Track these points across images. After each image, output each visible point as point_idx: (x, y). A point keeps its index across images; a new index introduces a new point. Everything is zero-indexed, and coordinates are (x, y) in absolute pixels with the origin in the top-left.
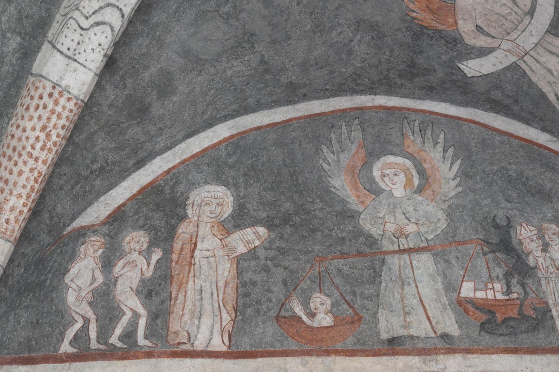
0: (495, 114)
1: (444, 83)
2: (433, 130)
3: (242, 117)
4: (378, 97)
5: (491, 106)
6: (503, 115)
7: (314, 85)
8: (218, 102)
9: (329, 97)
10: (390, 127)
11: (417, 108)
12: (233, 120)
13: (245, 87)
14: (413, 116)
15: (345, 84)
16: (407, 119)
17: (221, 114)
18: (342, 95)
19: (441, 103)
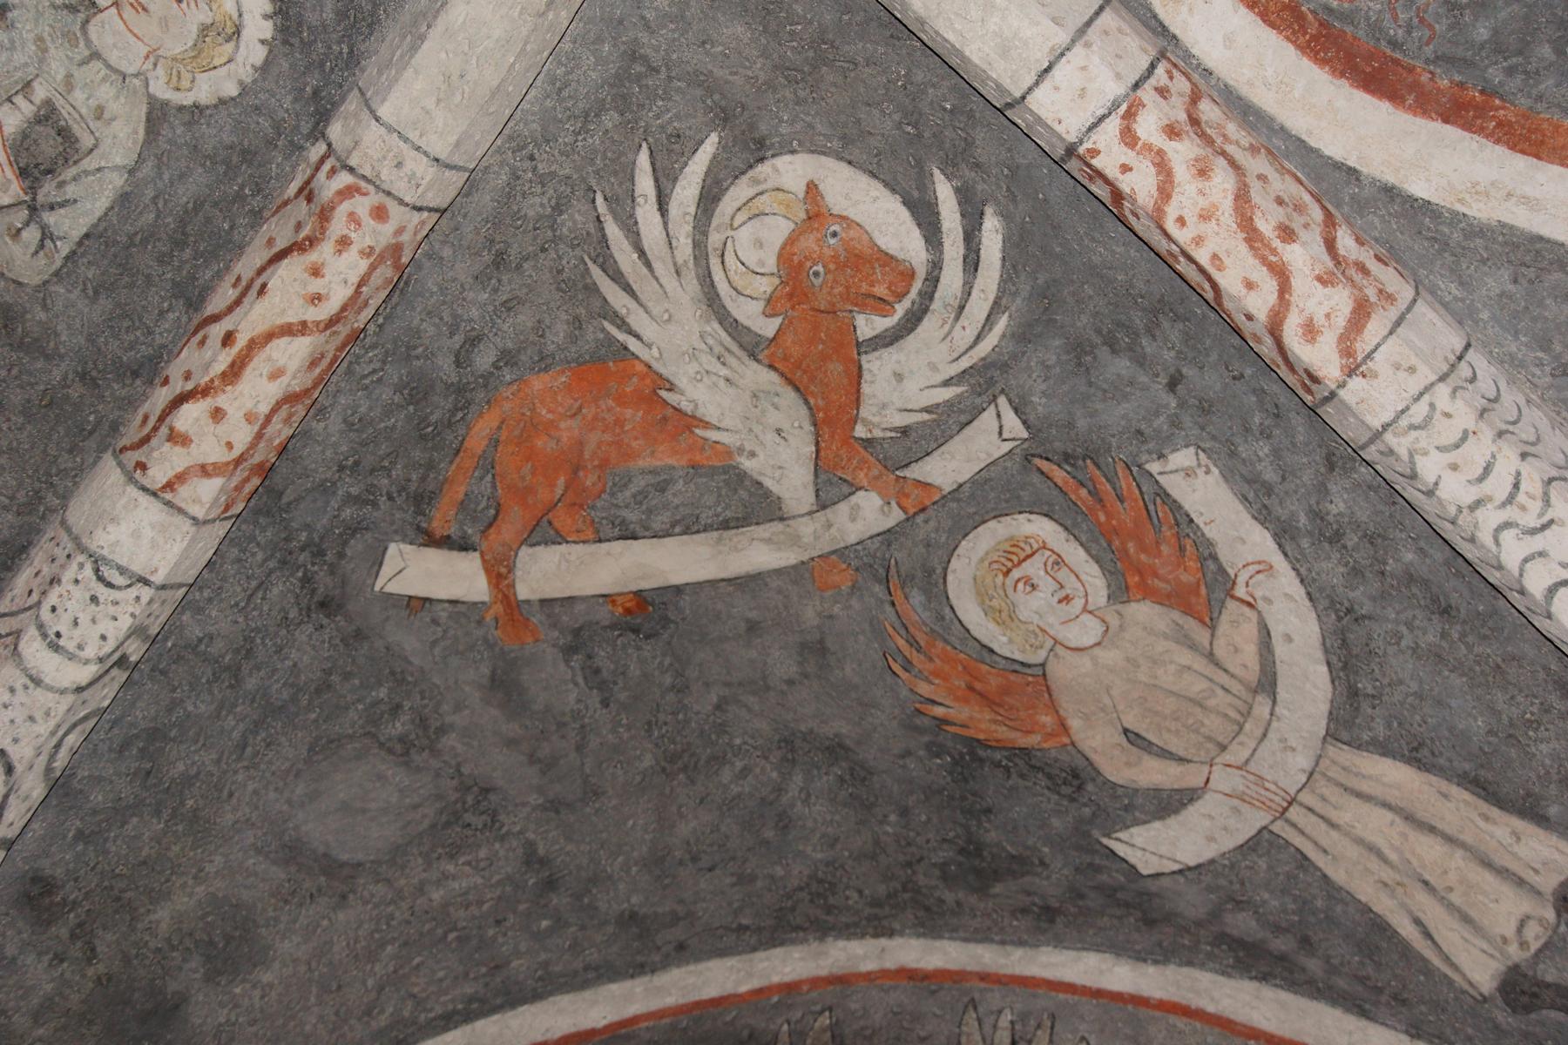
0: (1255, 985)
1: (1081, 896)
2: (1055, 1038)
3: (496, 1017)
4: (897, 941)
5: (1238, 960)
6: (1282, 987)
7: (700, 918)
8: (413, 979)
9: (754, 949)
10: (922, 1034)
11: (1009, 971)
12: (467, 1028)
13: (491, 932)
14: (995, 998)
15: (793, 909)
16: (975, 1008)
17: (431, 1010)
18: (793, 942)
19: (1085, 954)
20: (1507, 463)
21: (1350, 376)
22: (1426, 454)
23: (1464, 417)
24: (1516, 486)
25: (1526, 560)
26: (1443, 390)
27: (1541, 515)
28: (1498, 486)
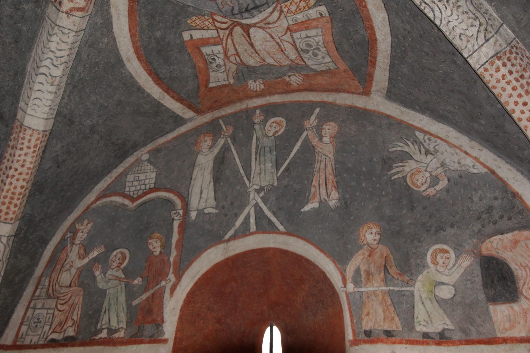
20: (65, 53)
21: (66, 13)
22: (57, 36)
23: (70, 41)
24: (61, 57)
25: (46, 66)
26: (74, 34)
27: (58, 64)
28: (59, 54)
